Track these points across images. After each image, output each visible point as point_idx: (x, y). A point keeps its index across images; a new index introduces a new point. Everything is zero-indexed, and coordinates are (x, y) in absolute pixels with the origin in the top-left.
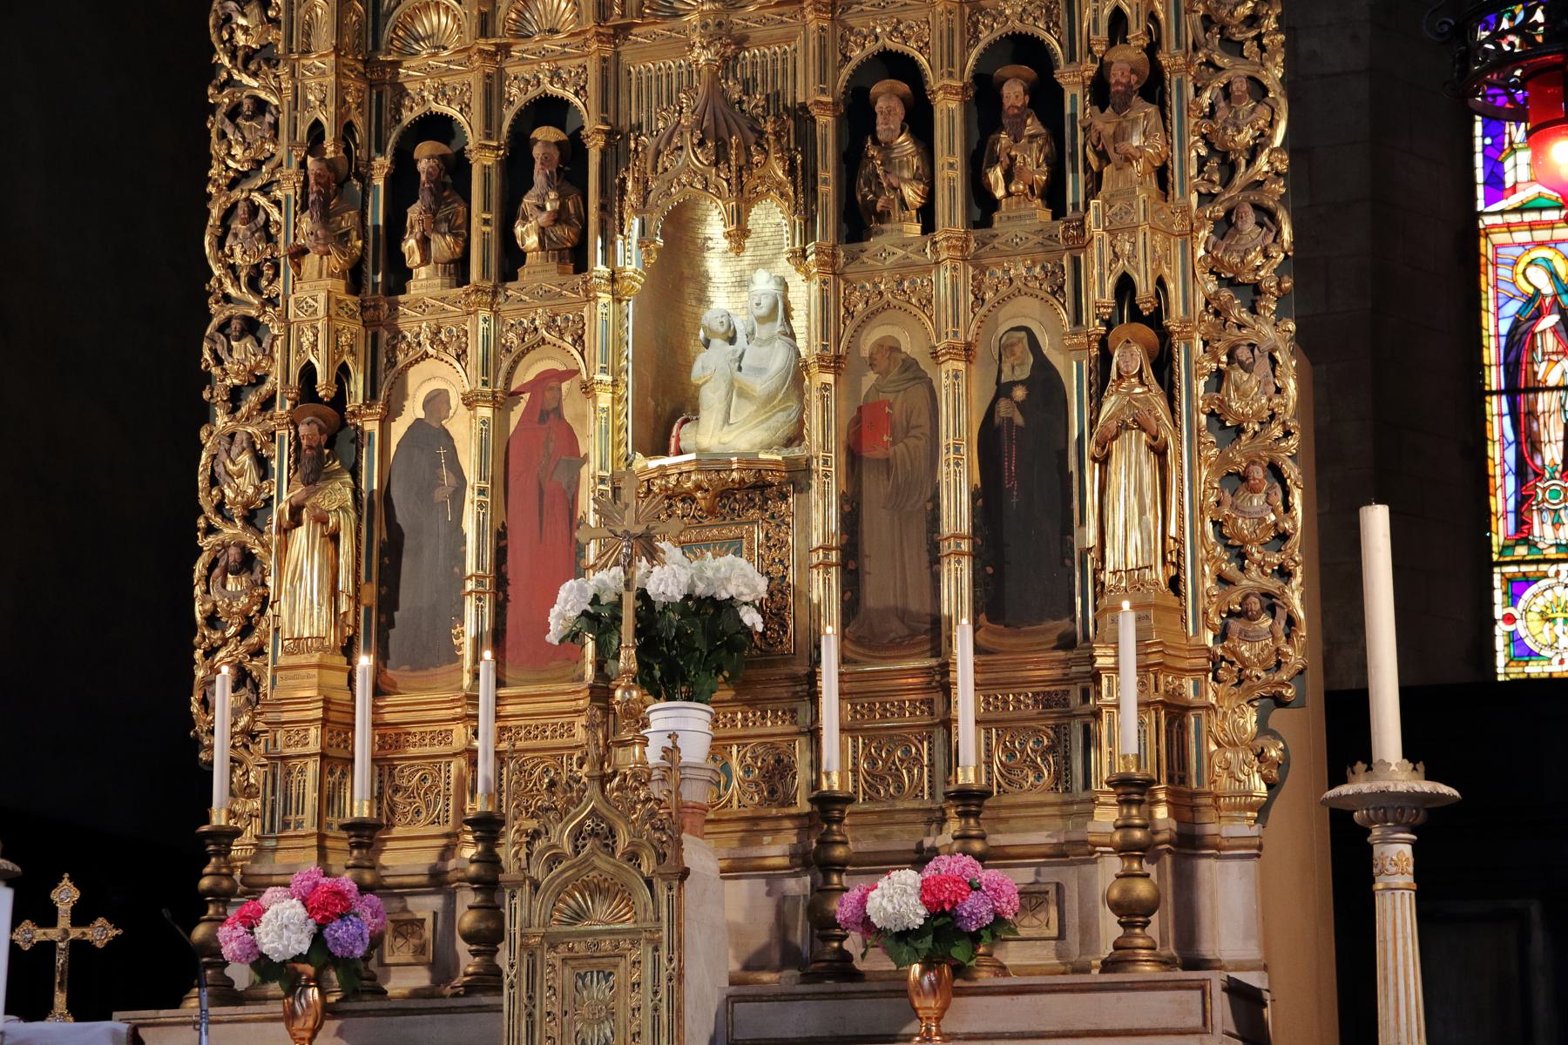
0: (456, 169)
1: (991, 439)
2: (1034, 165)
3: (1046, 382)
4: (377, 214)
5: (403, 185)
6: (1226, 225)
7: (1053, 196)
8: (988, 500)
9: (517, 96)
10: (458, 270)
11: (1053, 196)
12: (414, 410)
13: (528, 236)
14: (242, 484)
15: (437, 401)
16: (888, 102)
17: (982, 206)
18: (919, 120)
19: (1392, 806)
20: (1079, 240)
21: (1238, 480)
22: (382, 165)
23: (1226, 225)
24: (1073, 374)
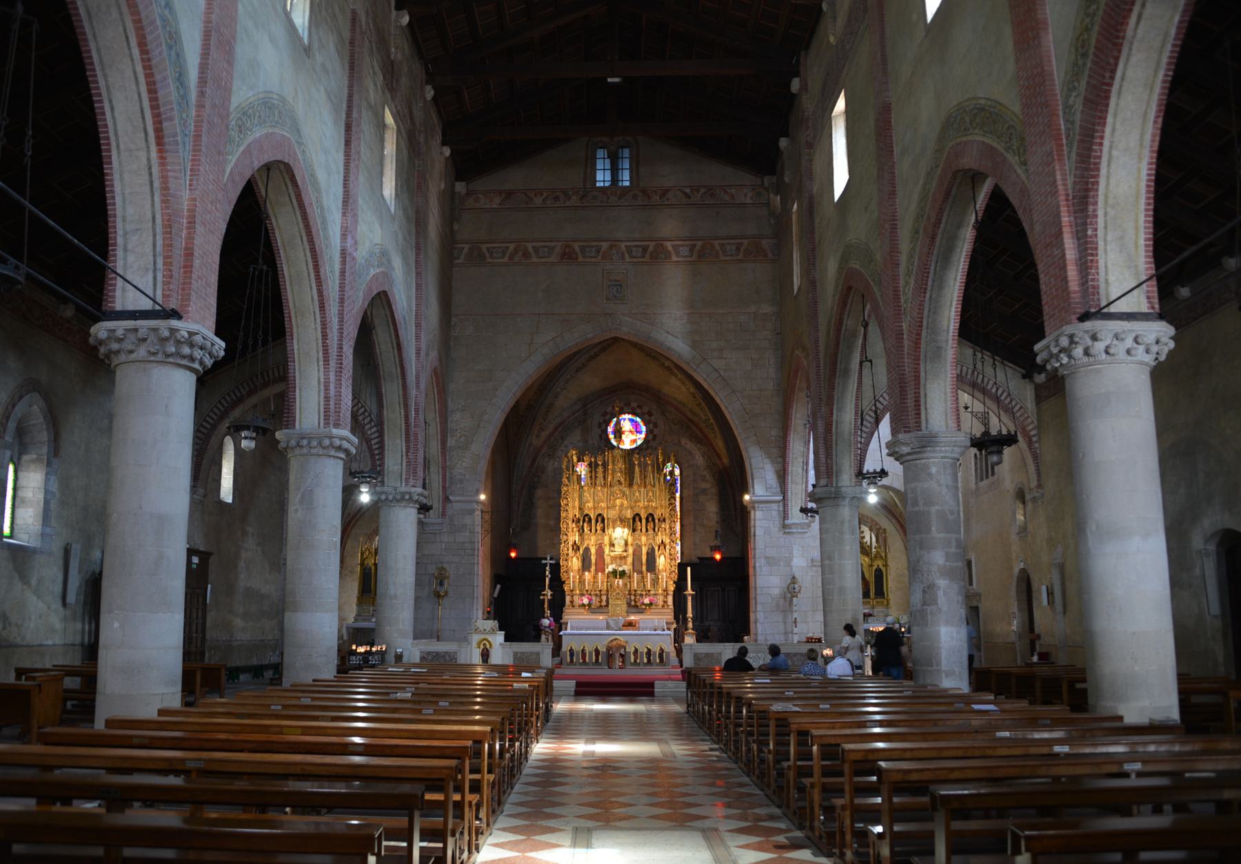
0: (590, 520)
1: (648, 553)
2: (652, 526)
3: (653, 549)
4: (581, 524)
5: (584, 521)
6: (671, 534)
7: (654, 530)
8: (647, 560)
9: (597, 513)
10: (591, 530)
11: (654, 530)
12: (586, 545)
13: (598, 528)
14: (566, 552)
15: (588, 545)
16: (637, 519)
17: (647, 531)
18: (640, 520)
19: (690, 595)
20: (657, 535)
21: (671, 560)
22: (582, 519)
23: (671, 534)
24: (656, 548)
